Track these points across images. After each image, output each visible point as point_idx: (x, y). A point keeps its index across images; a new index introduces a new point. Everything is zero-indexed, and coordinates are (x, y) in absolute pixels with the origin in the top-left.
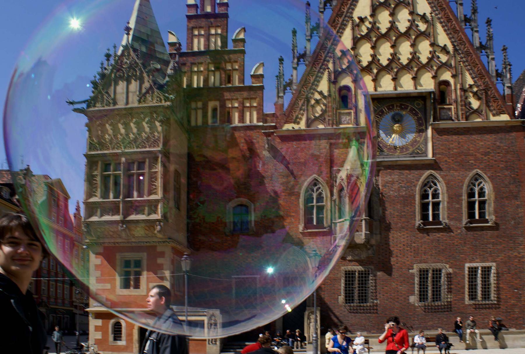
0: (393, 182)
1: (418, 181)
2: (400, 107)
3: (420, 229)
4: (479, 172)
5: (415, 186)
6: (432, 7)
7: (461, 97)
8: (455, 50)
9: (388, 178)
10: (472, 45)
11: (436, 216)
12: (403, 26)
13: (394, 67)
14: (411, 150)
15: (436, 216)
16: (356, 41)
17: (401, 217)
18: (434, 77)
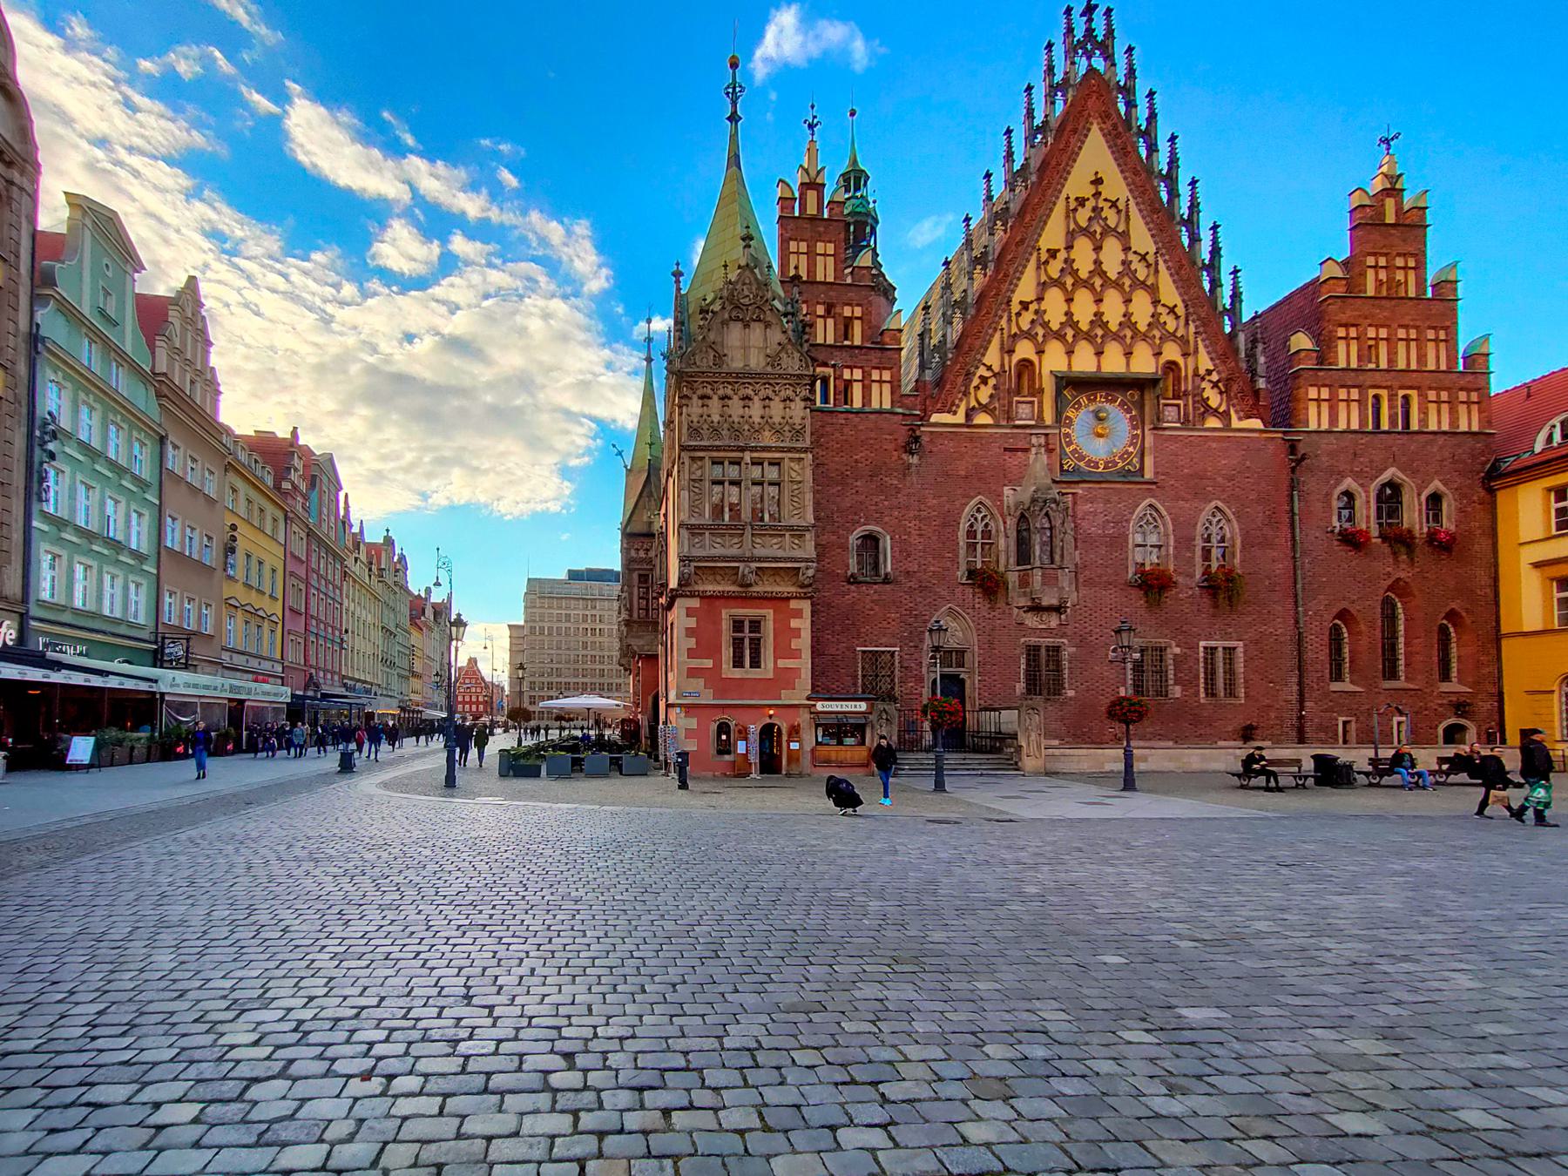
0: (1095, 514)
4: (1220, 504)
5: (1128, 521)
12: (1112, 269)
13: (1098, 334)
16: (1043, 287)
18: (1158, 354)
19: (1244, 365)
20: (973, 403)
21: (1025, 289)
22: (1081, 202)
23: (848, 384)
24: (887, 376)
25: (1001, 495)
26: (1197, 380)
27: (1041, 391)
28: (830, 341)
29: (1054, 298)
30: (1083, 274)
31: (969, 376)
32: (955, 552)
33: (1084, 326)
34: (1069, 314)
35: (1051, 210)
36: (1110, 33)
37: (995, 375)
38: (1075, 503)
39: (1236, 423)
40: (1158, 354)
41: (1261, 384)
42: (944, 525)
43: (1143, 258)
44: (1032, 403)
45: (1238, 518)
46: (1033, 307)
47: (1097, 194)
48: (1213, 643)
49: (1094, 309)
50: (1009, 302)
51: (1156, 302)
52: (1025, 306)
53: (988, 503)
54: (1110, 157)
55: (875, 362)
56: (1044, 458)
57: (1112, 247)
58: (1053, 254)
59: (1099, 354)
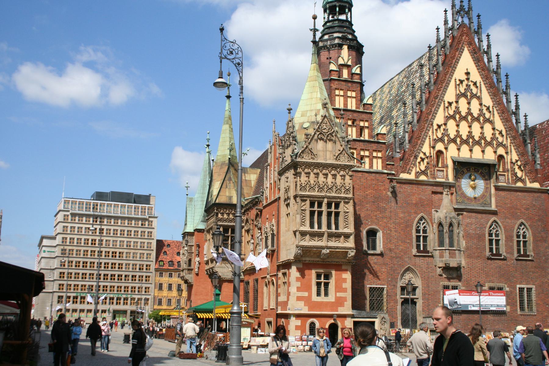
0: (471, 224)
1: (487, 224)
2: (474, 170)
3: (489, 259)
4: (523, 221)
5: (485, 227)
6: (493, 102)
7: (511, 168)
8: (507, 134)
9: (468, 221)
10: (517, 131)
11: (497, 249)
12: (476, 113)
13: (469, 141)
14: (481, 201)
15: (497, 249)
17: (477, 248)
18: (495, 152)
19: (530, 158)
20: (418, 170)
21: (439, 119)
22: (461, 82)
23: (362, 157)
24: (380, 155)
25: (431, 213)
26: (512, 165)
27: (447, 167)
28: (354, 137)
29: (451, 124)
30: (463, 114)
31: (416, 157)
32: (411, 240)
33: (464, 137)
34: (458, 131)
35: (449, 84)
36: (470, 8)
37: (427, 157)
38: (463, 218)
39: (529, 185)
40: (495, 152)
41: (538, 167)
42: (407, 226)
43: (488, 108)
44: (443, 171)
45: (531, 228)
46: (443, 127)
47: (468, 79)
48: (522, 286)
49: (468, 129)
50: (432, 124)
51: (494, 129)
52: (439, 126)
53: (425, 217)
54: (472, 63)
55: (374, 148)
56: (450, 196)
57: (475, 103)
58: (450, 104)
59: (471, 151)
